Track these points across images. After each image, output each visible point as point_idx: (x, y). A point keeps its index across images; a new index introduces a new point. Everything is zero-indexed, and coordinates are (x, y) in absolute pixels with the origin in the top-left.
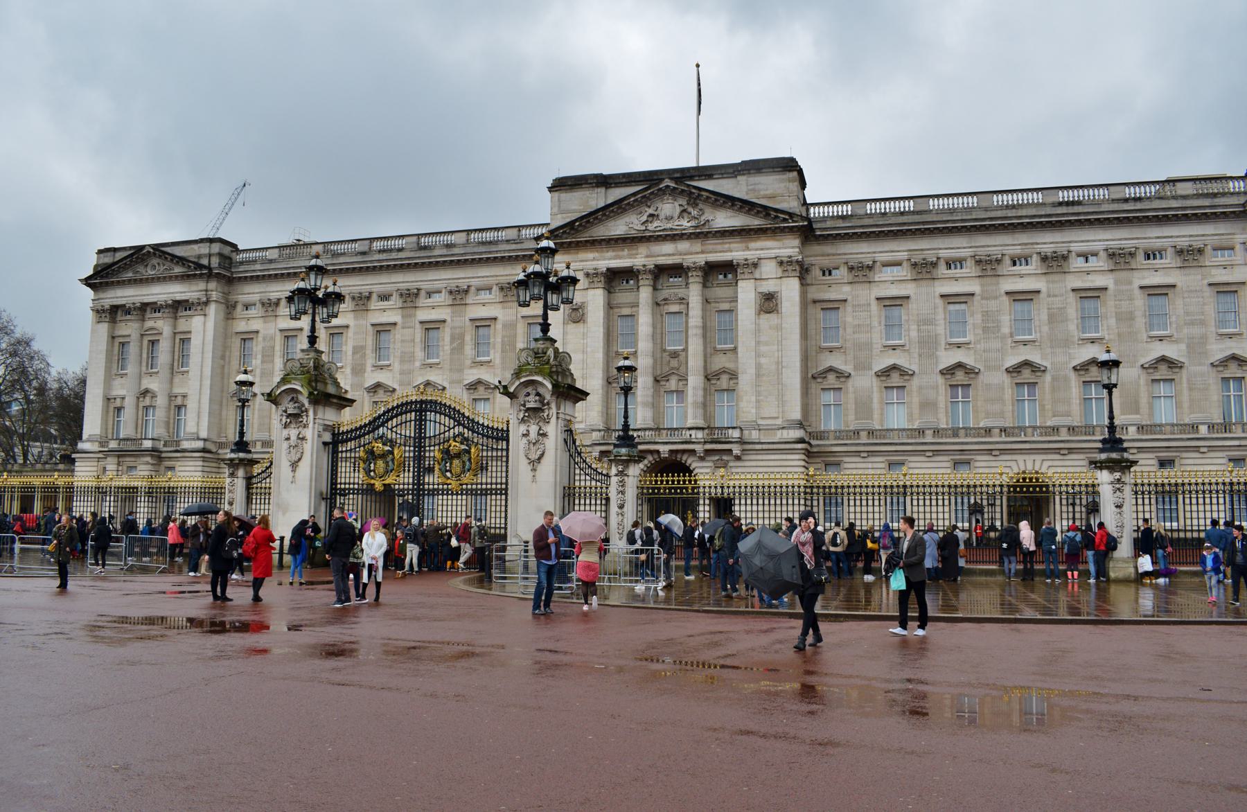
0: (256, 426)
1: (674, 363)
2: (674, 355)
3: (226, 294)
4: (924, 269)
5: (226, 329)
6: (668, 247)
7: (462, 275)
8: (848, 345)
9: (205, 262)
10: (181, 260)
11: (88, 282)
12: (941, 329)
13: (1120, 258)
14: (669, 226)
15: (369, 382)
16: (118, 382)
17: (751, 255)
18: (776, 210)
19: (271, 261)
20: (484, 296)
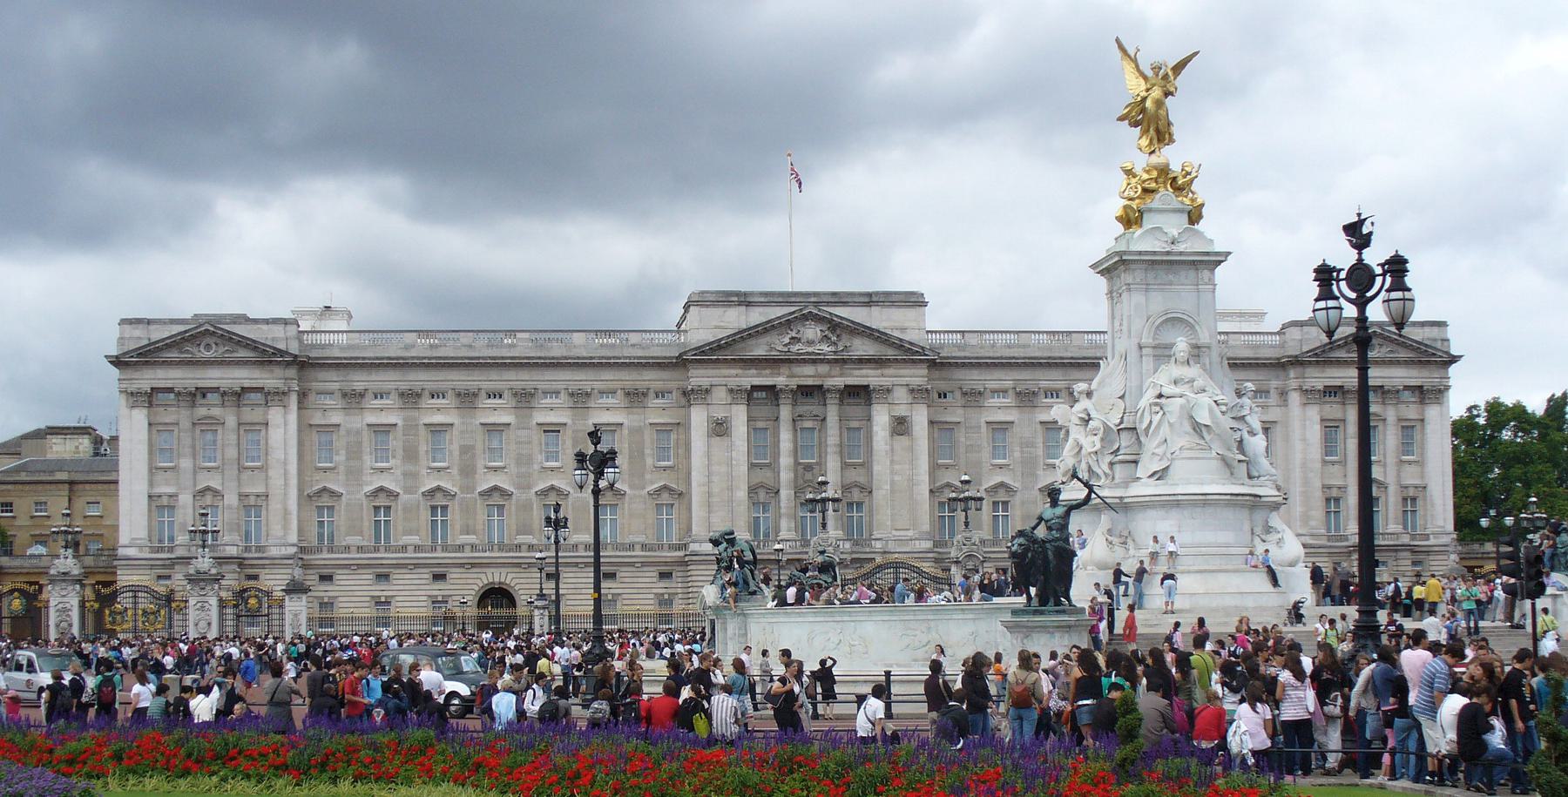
0: (343, 529)
2: (808, 468)
3: (300, 380)
4: (1027, 398)
5: (299, 417)
6: (809, 370)
9: (282, 346)
10: (252, 345)
11: (117, 362)
12: (1040, 452)
14: (810, 349)
15: (485, 487)
16: (160, 476)
17: (885, 382)
19: (350, 347)
20: (611, 401)
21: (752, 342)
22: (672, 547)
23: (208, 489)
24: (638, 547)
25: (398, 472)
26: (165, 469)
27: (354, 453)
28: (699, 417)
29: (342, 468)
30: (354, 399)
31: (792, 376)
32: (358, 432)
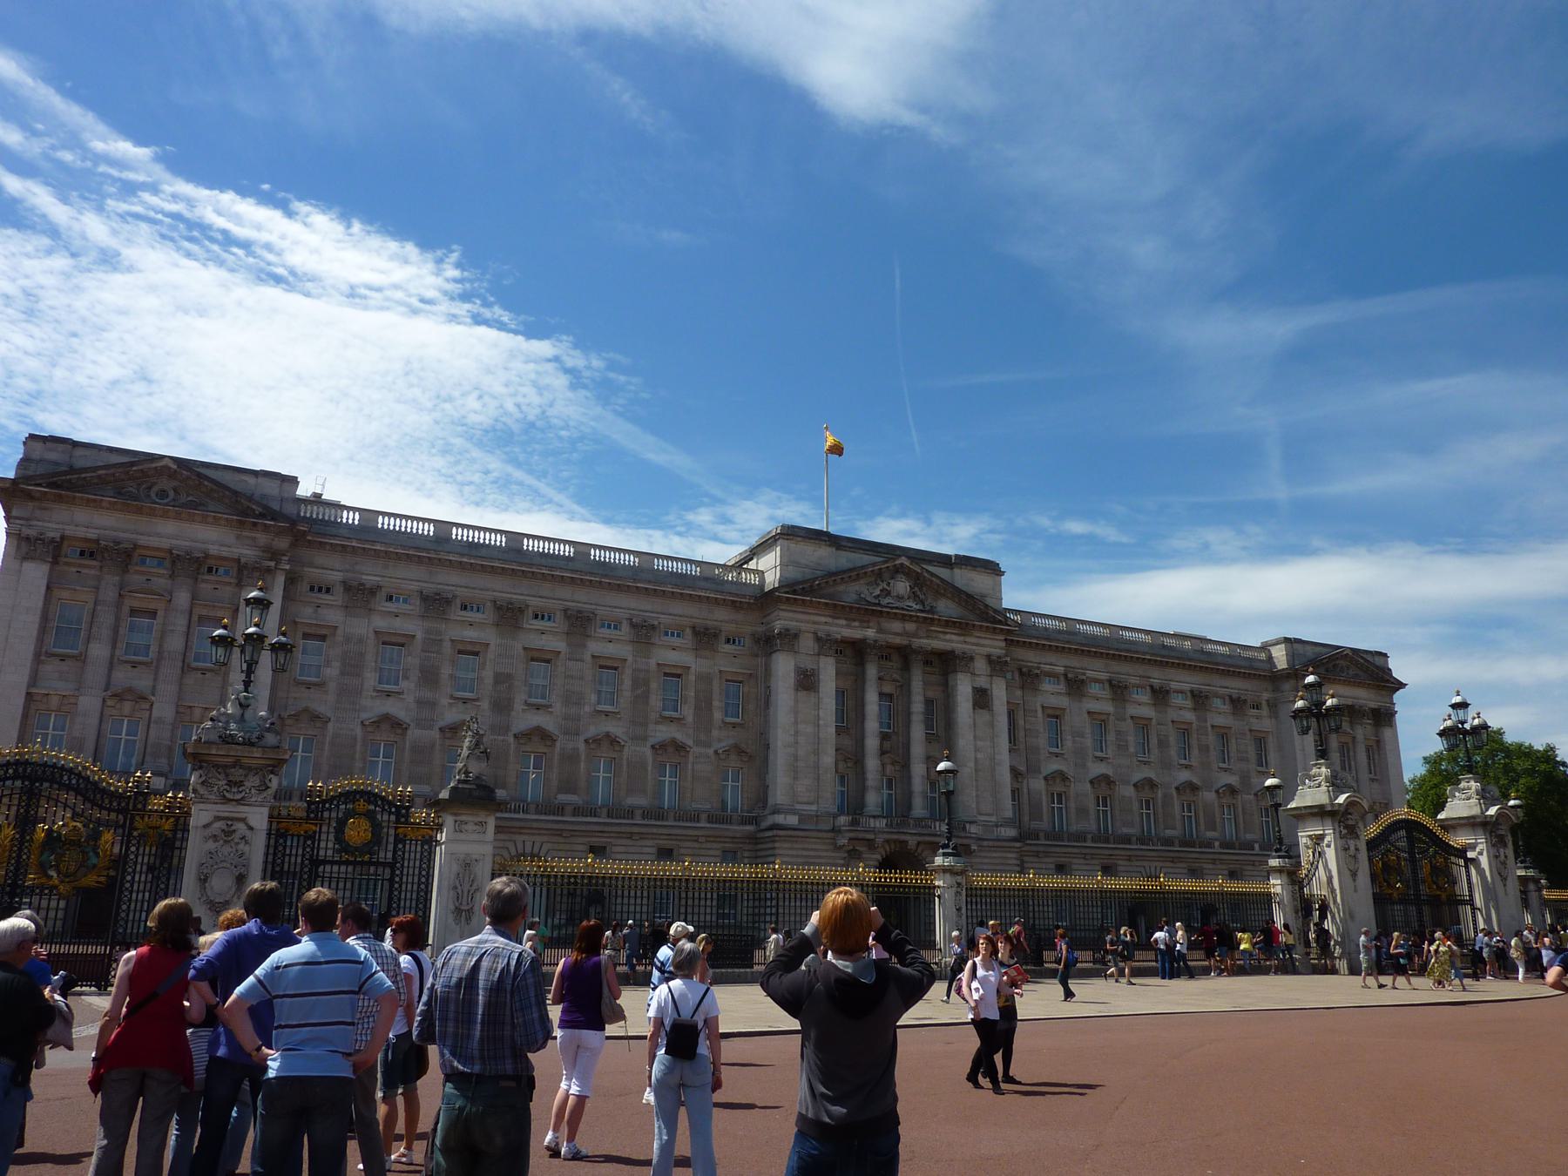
1: (887, 745)
4: (1076, 686)
6: (896, 626)
7: (649, 607)
8: (1022, 747)
9: (276, 506)
12: (1089, 742)
13: (1200, 699)
14: (898, 604)
16: (50, 668)
18: (995, 611)
20: (676, 641)
21: (841, 588)
22: (744, 821)
23: (130, 690)
24: (704, 816)
25: (410, 699)
26: (63, 658)
27: (353, 666)
28: (784, 666)
29: (332, 686)
30: (360, 596)
31: (880, 631)
32: (361, 641)
